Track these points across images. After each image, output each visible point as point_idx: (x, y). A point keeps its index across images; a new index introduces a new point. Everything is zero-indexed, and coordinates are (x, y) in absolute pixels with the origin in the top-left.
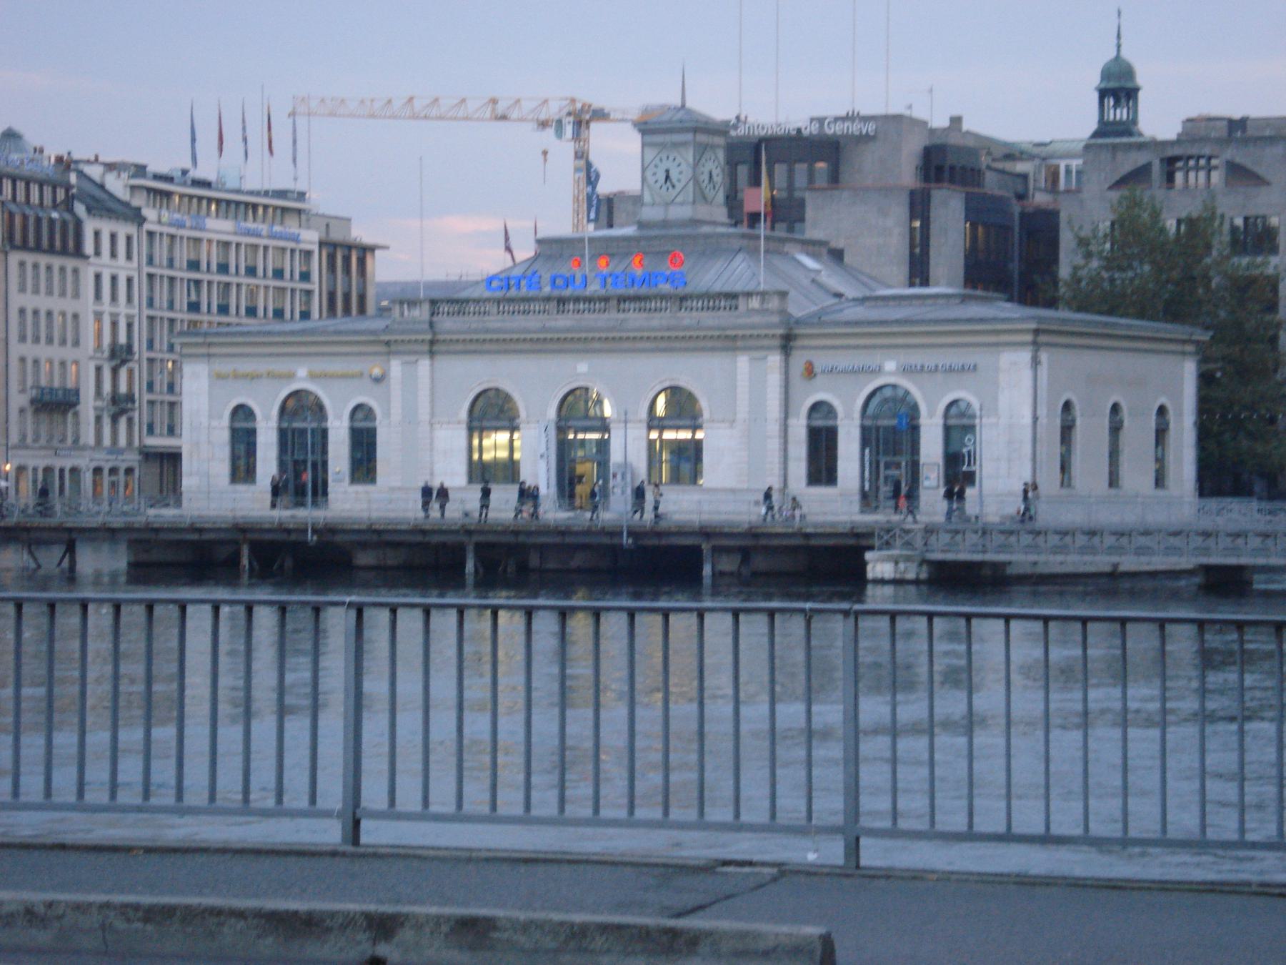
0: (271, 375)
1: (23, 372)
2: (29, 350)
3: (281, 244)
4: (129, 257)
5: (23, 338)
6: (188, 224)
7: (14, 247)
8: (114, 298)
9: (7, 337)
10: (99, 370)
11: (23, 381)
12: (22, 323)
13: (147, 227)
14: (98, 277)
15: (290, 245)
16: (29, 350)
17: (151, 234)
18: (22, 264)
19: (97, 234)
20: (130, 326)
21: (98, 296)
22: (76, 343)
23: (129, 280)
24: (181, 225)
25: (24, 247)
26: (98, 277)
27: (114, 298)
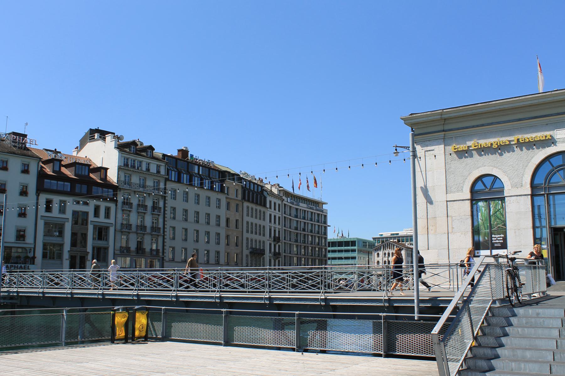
0: (520, 144)
1: (247, 243)
2: (250, 236)
3: (319, 212)
4: (279, 211)
5: (248, 232)
6: (295, 204)
7: (245, 200)
8: (275, 223)
9: (242, 231)
10: (270, 244)
11: (247, 246)
12: (248, 227)
13: (284, 202)
14: (270, 215)
15: (321, 213)
16: (250, 236)
17: (285, 205)
18: (248, 207)
19: (270, 202)
20: (279, 232)
21: (270, 221)
22: (264, 235)
23: (279, 218)
24: (293, 204)
25: (248, 201)
26: (270, 215)
27: (275, 223)
